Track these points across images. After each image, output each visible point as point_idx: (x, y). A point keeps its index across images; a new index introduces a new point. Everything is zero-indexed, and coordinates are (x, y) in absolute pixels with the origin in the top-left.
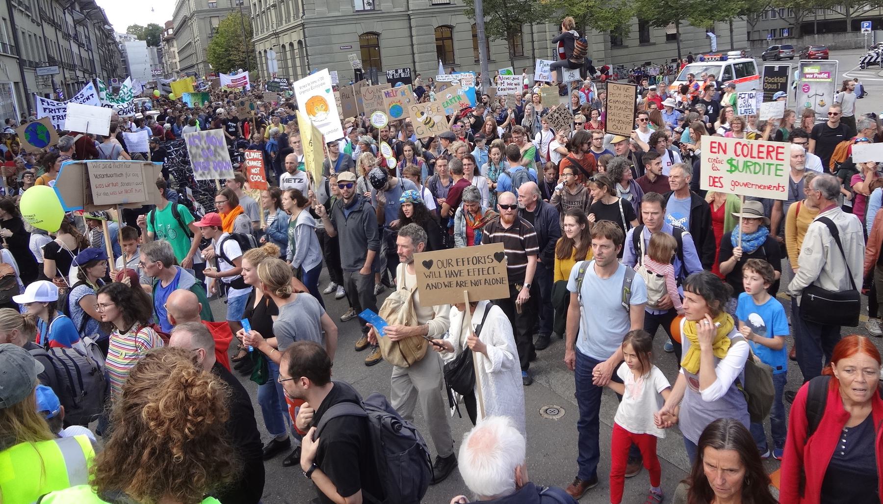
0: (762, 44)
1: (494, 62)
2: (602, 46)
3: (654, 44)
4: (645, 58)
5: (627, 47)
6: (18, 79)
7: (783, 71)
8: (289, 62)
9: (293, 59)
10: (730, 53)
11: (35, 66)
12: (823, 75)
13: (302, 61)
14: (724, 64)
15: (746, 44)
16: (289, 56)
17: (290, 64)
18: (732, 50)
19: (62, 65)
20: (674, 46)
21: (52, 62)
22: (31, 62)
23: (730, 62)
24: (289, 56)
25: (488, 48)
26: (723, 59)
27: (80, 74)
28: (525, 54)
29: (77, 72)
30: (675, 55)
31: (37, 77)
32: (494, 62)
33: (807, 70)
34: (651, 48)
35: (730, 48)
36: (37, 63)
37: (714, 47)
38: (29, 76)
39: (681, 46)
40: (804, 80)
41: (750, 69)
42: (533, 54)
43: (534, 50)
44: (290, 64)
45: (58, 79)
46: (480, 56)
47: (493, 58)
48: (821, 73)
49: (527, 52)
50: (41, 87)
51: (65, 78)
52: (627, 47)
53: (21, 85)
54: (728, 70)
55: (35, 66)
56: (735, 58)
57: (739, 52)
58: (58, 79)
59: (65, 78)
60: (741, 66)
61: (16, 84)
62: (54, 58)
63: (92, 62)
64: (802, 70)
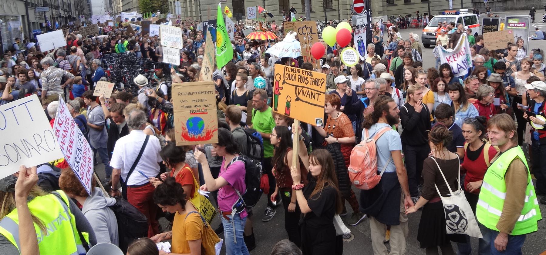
0: (481, 5)
1: (314, 12)
2: (381, 4)
3: (413, 4)
4: (408, 12)
5: (396, 5)
6: (24, 13)
7: (495, 22)
8: (189, 8)
9: (191, 7)
10: (461, 10)
11: (35, 6)
12: (521, 25)
13: (196, 9)
14: (457, 17)
15: (470, 5)
16: (188, 5)
17: (189, 10)
18: (462, 8)
19: (51, 6)
20: (426, 5)
21: (45, 4)
22: (32, 4)
23: (461, 15)
24: (188, 5)
25: (310, 3)
26: (457, 13)
27: (61, 12)
28: (334, 8)
29: (60, 11)
30: (426, 10)
31: (35, 13)
32: (314, 12)
33: (510, 21)
34: (412, 6)
35: (461, 7)
36: (36, 5)
37: (451, 7)
38: (31, 12)
39: (430, 5)
40: (509, 27)
41: (474, 20)
42: (338, 8)
43: (339, 5)
44: (189, 10)
45: (48, 15)
46: (306, 8)
47: (313, 9)
48: (519, 24)
49: (335, 7)
50: (37, 19)
51: (53, 14)
52: (396, 5)
53: (26, 17)
54: (460, 21)
55: (35, 6)
56: (464, 13)
57: (467, 10)
58: (48, 15)
59: (53, 14)
60: (468, 18)
61: (23, 16)
62: (46, 2)
63: (69, 5)
64: (507, 21)
